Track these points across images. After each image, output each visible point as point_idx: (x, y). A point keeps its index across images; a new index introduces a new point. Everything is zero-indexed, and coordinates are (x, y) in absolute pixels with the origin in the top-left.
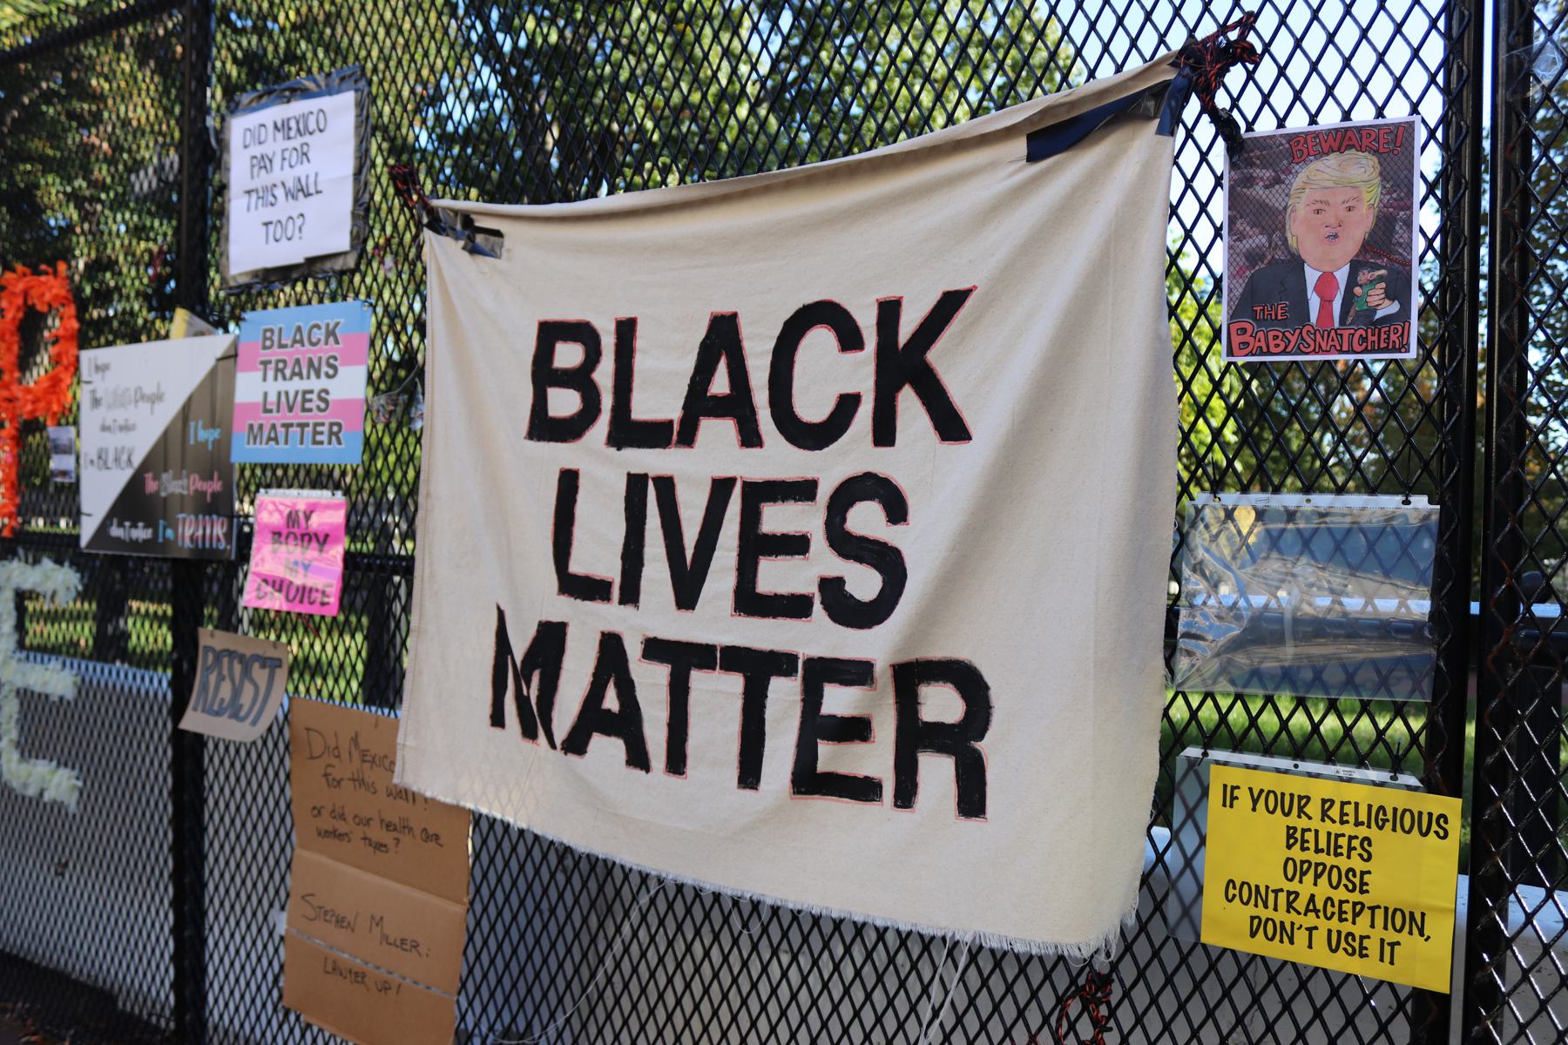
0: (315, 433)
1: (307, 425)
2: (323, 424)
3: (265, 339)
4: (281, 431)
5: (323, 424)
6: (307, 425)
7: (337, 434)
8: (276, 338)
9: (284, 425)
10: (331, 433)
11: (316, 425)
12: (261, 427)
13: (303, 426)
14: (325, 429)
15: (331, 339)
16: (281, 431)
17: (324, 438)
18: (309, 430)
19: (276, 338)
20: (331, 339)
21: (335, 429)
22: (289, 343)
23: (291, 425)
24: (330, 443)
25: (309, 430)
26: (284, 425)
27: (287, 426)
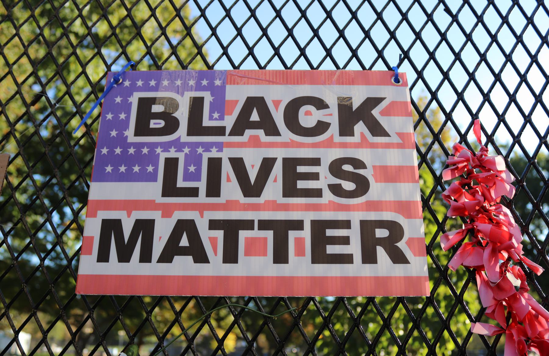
1: (298, 225)
2: (347, 224)
5: (347, 224)
6: (298, 225)
15: (360, 128)
20: (360, 128)
21: (381, 233)
22: (229, 122)
23: (248, 225)
26: (214, 225)
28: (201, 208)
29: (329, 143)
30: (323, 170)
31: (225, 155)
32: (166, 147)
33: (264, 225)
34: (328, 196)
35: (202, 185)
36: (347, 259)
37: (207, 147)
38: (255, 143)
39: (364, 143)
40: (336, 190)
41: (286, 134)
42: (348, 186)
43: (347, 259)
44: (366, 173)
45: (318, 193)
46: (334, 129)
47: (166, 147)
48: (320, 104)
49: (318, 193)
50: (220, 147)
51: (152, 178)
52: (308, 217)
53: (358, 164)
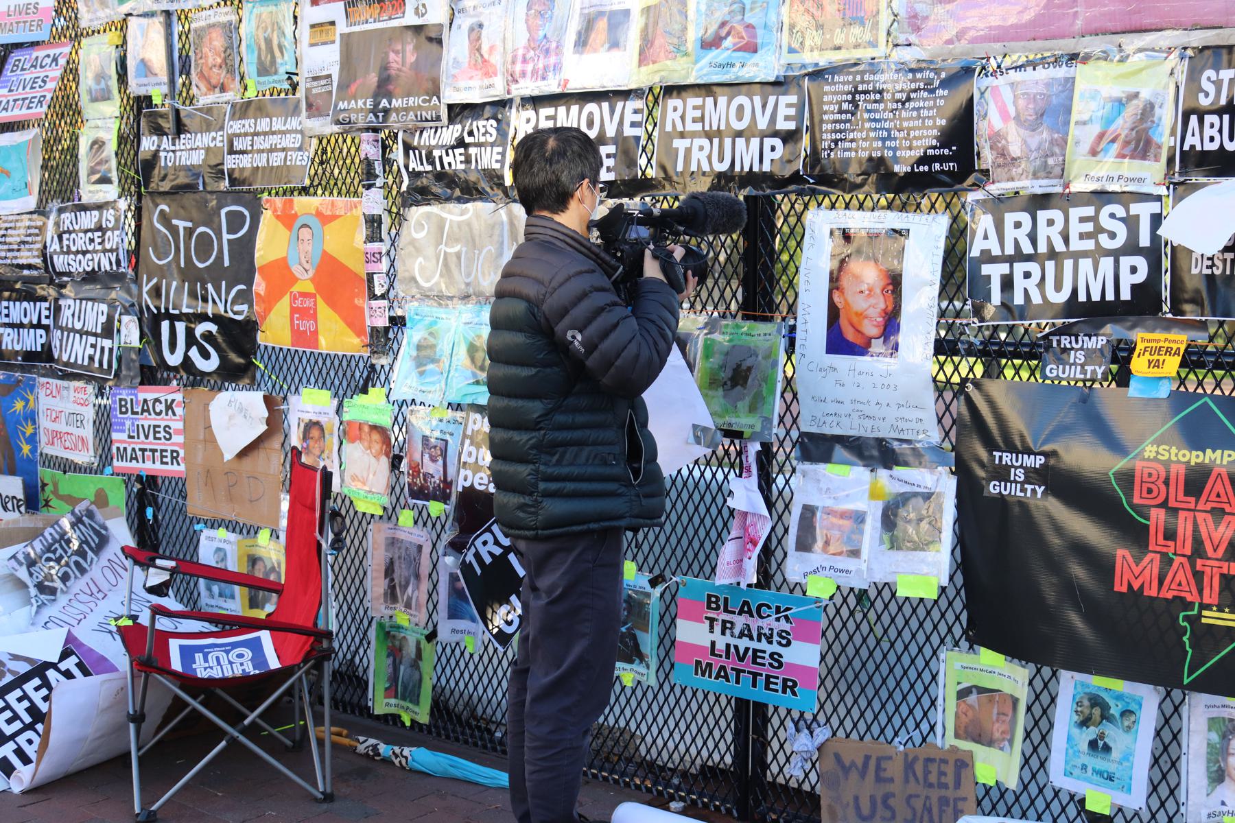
0: (162, 457)
3: (121, 406)
4: (139, 453)
7: (176, 458)
8: (129, 406)
9: (140, 450)
10: (173, 458)
11: (162, 451)
12: (125, 449)
13: (154, 451)
14: (168, 454)
16: (139, 453)
17: (168, 460)
18: (158, 454)
19: (129, 406)
22: (139, 410)
25: (158, 454)
26: (140, 450)
27: (143, 450)
29: (162, 419)
30: (161, 429)
31: (140, 423)
33: (151, 450)
34: (163, 440)
38: (146, 419)
41: (153, 416)
43: (166, 463)
51: (124, 431)
52: (159, 448)
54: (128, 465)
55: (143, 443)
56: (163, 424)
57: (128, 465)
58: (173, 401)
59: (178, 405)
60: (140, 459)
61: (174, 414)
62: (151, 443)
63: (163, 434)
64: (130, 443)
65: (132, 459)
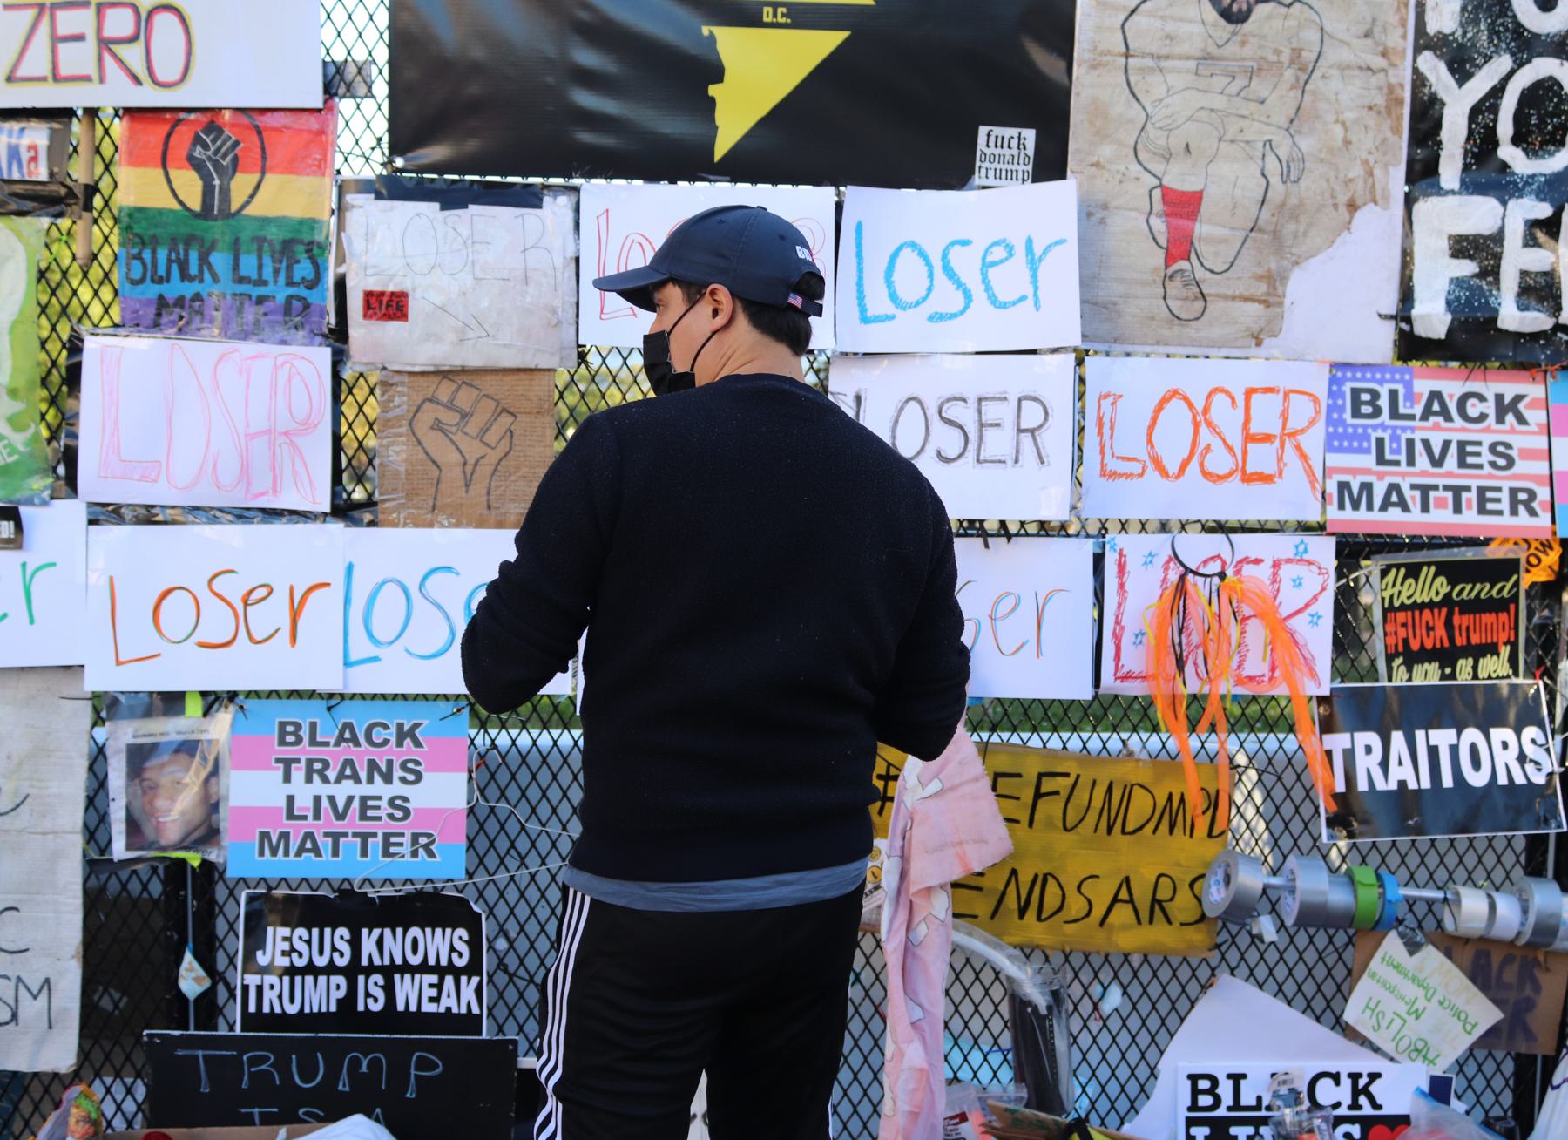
5: (1499, 489)
8: (1384, 402)
11: (1482, 491)
13: (1457, 491)
14: (1505, 496)
15: (1510, 418)
17: (1505, 505)
19: (1384, 402)
20: (1510, 418)
22: (1418, 410)
23: (1436, 487)
24: (1514, 512)
28: (1403, 475)
30: (1484, 449)
32: (1375, 428)
33: (1446, 488)
34: (1487, 469)
35: (1403, 458)
36: (1500, 513)
37: (1404, 429)
38: (1436, 427)
39: (1512, 431)
40: (1493, 465)
41: (1458, 422)
42: (1501, 462)
43: (1500, 513)
44: (1514, 453)
45: (1480, 466)
46: (1492, 418)
47: (1375, 428)
48: (1482, 398)
49: (1480, 466)
50: (1413, 429)
52: (1474, 484)
53: (1508, 446)
54: (1376, 515)
55: (1424, 473)
56: (1487, 439)
57: (1376, 515)
58: (1518, 398)
59: (1532, 406)
60: (1415, 506)
61: (1521, 420)
62: (1449, 474)
63: (1486, 457)
64: (1381, 476)
65: (1384, 507)
